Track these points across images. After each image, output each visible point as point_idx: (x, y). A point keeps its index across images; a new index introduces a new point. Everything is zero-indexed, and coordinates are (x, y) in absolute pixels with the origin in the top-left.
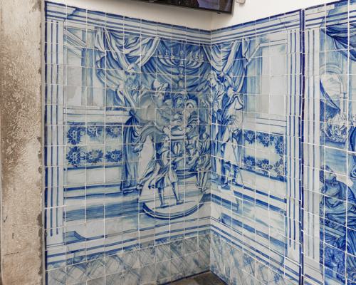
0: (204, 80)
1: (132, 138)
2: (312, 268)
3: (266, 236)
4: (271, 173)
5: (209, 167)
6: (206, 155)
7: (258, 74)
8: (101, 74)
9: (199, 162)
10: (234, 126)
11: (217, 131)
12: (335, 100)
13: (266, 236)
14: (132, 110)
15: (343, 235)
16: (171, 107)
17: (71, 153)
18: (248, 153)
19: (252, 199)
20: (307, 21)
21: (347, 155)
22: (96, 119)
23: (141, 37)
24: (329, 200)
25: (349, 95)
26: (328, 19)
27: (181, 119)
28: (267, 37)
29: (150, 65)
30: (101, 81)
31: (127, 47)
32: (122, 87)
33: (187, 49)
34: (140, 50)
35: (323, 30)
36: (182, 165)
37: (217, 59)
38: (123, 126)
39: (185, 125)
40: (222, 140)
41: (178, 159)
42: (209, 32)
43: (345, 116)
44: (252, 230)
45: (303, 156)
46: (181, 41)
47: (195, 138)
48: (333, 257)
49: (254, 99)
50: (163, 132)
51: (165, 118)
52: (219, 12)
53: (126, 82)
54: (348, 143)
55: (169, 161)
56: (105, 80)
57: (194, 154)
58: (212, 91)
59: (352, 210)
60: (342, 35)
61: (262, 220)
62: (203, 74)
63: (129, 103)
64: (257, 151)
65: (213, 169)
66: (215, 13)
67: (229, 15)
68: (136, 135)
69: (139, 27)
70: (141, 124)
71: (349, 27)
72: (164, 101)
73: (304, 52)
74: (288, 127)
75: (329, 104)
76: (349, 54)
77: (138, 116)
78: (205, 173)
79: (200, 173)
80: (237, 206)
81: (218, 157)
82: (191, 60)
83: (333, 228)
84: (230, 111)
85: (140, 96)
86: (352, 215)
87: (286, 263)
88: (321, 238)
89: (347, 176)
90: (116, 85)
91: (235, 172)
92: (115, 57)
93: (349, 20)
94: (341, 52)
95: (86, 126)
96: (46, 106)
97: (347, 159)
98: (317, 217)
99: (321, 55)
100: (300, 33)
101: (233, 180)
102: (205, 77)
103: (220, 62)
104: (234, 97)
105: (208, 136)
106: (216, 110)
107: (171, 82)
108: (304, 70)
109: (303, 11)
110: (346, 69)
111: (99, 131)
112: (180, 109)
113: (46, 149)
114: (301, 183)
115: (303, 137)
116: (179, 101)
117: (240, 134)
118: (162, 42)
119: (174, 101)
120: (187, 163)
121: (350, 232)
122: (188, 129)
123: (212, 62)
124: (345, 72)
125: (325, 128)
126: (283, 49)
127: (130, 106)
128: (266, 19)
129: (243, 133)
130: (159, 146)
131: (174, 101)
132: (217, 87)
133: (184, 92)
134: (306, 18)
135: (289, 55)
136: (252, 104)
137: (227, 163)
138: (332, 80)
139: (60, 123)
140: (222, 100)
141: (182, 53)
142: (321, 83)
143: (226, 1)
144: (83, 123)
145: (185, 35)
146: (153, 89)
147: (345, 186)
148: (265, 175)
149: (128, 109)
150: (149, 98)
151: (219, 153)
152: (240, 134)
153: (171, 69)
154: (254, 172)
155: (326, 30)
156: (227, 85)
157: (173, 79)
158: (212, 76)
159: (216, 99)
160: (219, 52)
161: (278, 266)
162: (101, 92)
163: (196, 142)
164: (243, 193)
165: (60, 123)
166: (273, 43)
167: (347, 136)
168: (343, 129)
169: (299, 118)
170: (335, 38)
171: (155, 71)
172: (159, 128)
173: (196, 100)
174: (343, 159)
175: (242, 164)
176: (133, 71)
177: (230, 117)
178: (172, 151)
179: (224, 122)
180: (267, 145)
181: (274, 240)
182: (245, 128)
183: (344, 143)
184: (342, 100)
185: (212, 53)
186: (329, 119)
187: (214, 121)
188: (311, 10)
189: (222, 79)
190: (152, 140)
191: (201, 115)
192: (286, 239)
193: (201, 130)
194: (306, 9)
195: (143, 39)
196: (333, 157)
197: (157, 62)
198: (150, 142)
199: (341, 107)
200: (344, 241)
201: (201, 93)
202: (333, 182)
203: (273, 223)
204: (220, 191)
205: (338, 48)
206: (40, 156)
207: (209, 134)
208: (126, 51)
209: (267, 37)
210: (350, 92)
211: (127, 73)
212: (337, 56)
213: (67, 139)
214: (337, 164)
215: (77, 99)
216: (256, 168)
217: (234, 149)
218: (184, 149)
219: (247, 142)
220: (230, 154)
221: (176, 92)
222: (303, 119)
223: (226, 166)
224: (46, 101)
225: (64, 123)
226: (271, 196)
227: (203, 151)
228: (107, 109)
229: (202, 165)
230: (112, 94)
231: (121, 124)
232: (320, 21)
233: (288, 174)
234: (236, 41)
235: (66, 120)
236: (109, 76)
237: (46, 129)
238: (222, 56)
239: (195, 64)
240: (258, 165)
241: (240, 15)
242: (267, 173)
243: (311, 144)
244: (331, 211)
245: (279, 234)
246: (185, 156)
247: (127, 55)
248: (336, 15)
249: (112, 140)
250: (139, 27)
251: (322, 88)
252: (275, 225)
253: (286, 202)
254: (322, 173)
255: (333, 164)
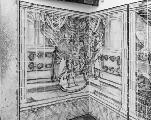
0: (86, 34)
1: (56, 58)
2: (132, 113)
3: (113, 99)
4: (115, 73)
5: (88, 70)
6: (88, 65)
7: (110, 31)
8: (43, 31)
9: (85, 68)
10: (99, 53)
11: (92, 55)
12: (142, 42)
13: (113, 99)
14: (56, 46)
15: (146, 99)
16: (72, 45)
17: (30, 65)
18: (105, 65)
19: (107, 84)
20: (130, 9)
21: (147, 65)
22: (40, 50)
23: (60, 16)
24: (139, 84)
25: (148, 40)
26: (139, 8)
27: (77, 50)
28: (113, 16)
29: (63, 27)
30: (43, 34)
31: (54, 20)
32: (51, 37)
33: (79, 21)
34: (59, 21)
35: (137, 13)
36: (77, 70)
37: (92, 25)
38: (52, 53)
39: (78, 53)
40: (94, 59)
41: (76, 67)
42: (89, 13)
43: (146, 49)
44: (107, 97)
45: (128, 65)
46: (76, 17)
47: (83, 58)
48: (141, 108)
49: (108, 42)
50: (69, 56)
51: (70, 50)
52: (93, 5)
53: (53, 35)
54: (147, 60)
55: (71, 68)
56: (44, 34)
57: (82, 65)
58: (90, 38)
59: (149, 88)
60: (145, 15)
61: (111, 93)
62: (86, 31)
63: (55, 43)
64: (109, 63)
65: (90, 71)
66: (91, 6)
67: (97, 6)
68: (58, 57)
69: (59, 12)
70: (60, 52)
71: (148, 11)
72: (69, 43)
73: (129, 22)
74: (122, 53)
75: (139, 44)
76: (148, 23)
77: (59, 49)
78: (87, 73)
79: (85, 73)
80: (101, 87)
81: (93, 66)
82: (81, 25)
83: (141, 96)
84: (98, 47)
85: (59, 41)
86: (149, 90)
87: (121, 111)
88: (136, 100)
89: (147, 74)
90: (49, 36)
91: (100, 73)
92: (49, 24)
93: (148, 8)
94: (145, 22)
95: (36, 53)
96: (19, 45)
97: (147, 67)
98: (134, 91)
99: (136, 23)
100: (127, 14)
101: (99, 76)
102: (87, 32)
103: (93, 26)
104: (99, 41)
105: (88, 57)
106: (91, 46)
107: (73, 35)
108: (129, 29)
109: (129, 5)
110: (147, 29)
111: (42, 55)
112: (76, 46)
113: (19, 63)
114: (128, 77)
115: (128, 58)
116: (76, 43)
117: (102, 56)
118: (69, 18)
119: (74, 43)
120: (79, 69)
121: (149, 98)
122: (80, 55)
123: (89, 26)
124: (146, 31)
125: (138, 54)
126: (120, 20)
127: (55, 45)
128: (113, 8)
129: (103, 56)
130: (67, 61)
131: (74, 43)
132: (92, 37)
133: (78, 39)
134: (130, 8)
135: (123, 23)
136: (106, 44)
137: (96, 69)
138: (141, 34)
139: (26, 52)
140: (94, 42)
141: (77, 22)
142: (136, 35)
143: (96, 0)
144: (36, 52)
145: (78, 15)
146: (65, 37)
147: (146, 78)
148: (112, 74)
149: (54, 46)
150: (63, 41)
151: (93, 65)
152: (102, 56)
153: (72, 29)
154: (108, 72)
155: (138, 13)
156: (96, 36)
157: (73, 33)
158: (90, 32)
159: (91, 42)
160: (93, 22)
161: (118, 112)
162: (43, 39)
163: (83, 60)
164: (103, 81)
165: (26, 52)
166: (116, 18)
167: (147, 58)
168: (145, 54)
169: (127, 50)
170: (142, 16)
171: (66, 30)
172: (67, 54)
173: (83, 42)
174: (145, 67)
175: (102, 69)
176: (56, 30)
177: (98, 49)
178: (73, 64)
179: (95, 51)
180: (113, 61)
181: (116, 101)
182: (104, 54)
183: (146, 60)
184: (145, 42)
185: (90, 22)
186: (140, 50)
187: (91, 51)
188: (132, 4)
189: (94, 34)
190: (65, 59)
191: (85, 49)
192: (121, 101)
193: (85, 55)
194: (130, 4)
195: (60, 17)
196: (141, 66)
197: (66, 26)
198: (64, 60)
199: (145, 45)
200: (146, 102)
201: (85, 39)
202: (141, 77)
203: (115, 94)
204: (93, 81)
205: (143, 20)
206: (17, 66)
207: (88, 56)
208: (53, 22)
209: (113, 16)
210: (148, 39)
211: (54, 31)
212: (143, 24)
213: (28, 59)
214: (143, 69)
215: (32, 42)
216: (109, 71)
217: (99, 63)
218: (78, 63)
219: (105, 60)
220: (98, 65)
221: (75, 39)
222: (128, 50)
223: (96, 70)
224: (19, 43)
225: (27, 52)
226: (115, 83)
227: (86, 64)
228: (45, 46)
229: (86, 69)
230: (47, 40)
231: (51, 52)
232: (136, 9)
233: (122, 73)
234: (100, 18)
235: (28, 51)
236: (46, 32)
237: (19, 54)
238: (94, 24)
239: (82, 27)
240: (109, 69)
241: (102, 6)
242: (113, 73)
243: (132, 61)
244: (140, 89)
245: (118, 99)
246: (78, 66)
247: (54, 23)
248: (142, 6)
249: (47, 59)
250: (59, 12)
251: (136, 37)
252: (117, 95)
253: (121, 85)
254: (136, 73)
255: (141, 69)
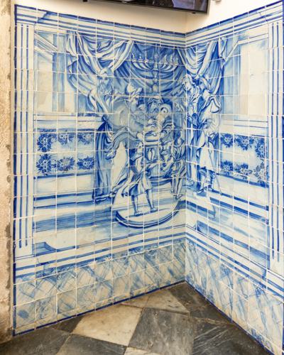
0: (178, 84)
3: (246, 246)
4: (250, 178)
7: (236, 74)
9: (174, 168)
11: (192, 135)
13: (246, 246)
19: (230, 206)
28: (246, 34)
36: (156, 172)
37: (192, 62)
39: (159, 130)
41: (152, 165)
42: (184, 35)
44: (230, 239)
49: (232, 101)
57: (169, 160)
58: (186, 94)
61: (241, 229)
64: (234, 154)
65: (189, 175)
78: (180, 179)
80: (214, 213)
81: (194, 162)
84: (206, 115)
91: (212, 178)
101: (210, 186)
102: (180, 81)
104: (210, 100)
105: (183, 142)
106: (191, 114)
117: (216, 138)
120: (161, 169)
122: (163, 134)
123: (186, 65)
126: (263, 44)
128: (244, 14)
129: (220, 136)
132: (192, 91)
135: (271, 51)
137: (202, 168)
140: (198, 104)
148: (244, 180)
151: (195, 159)
152: (217, 137)
156: (202, 88)
158: (187, 80)
159: (191, 103)
160: (194, 54)
163: (170, 147)
164: (220, 200)
173: (171, 104)
175: (218, 170)
177: (206, 121)
179: (199, 126)
180: (246, 148)
182: (222, 131)
185: (187, 56)
187: (189, 125)
189: (197, 82)
191: (175, 120)
192: (268, 250)
193: (176, 135)
201: (175, 97)
204: (195, 198)
209: (246, 34)
216: (234, 174)
217: (210, 154)
219: (224, 146)
220: (206, 159)
223: (201, 171)
226: (251, 203)
227: (179, 157)
229: (177, 171)
233: (270, 179)
234: (212, 42)
238: (197, 58)
241: (216, 13)
242: (246, 178)
246: (160, 162)
253: (268, 210)
